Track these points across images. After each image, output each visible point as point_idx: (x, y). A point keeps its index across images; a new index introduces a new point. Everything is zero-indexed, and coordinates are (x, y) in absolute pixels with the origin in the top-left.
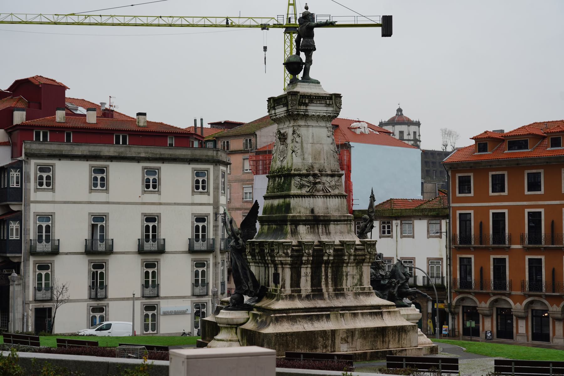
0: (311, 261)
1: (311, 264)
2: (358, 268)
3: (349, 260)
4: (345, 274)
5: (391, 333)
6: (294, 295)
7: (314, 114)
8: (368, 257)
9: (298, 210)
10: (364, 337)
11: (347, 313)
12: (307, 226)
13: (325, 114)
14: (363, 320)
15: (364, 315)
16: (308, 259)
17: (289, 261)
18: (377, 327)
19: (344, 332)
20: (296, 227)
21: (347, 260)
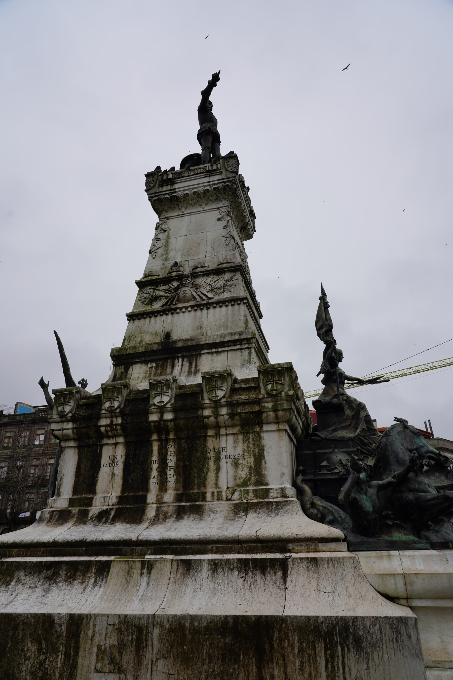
0: (119, 427)
1: (125, 437)
2: (248, 439)
3: (216, 418)
4: (212, 455)
5: (292, 646)
6: (70, 512)
8: (270, 405)
9: (139, 339)
11: (165, 560)
12: (147, 364)
14: (212, 585)
15: (220, 570)
16: (112, 422)
17: (70, 432)
18: (236, 618)
19: (110, 628)
20: (127, 370)
21: (212, 419)
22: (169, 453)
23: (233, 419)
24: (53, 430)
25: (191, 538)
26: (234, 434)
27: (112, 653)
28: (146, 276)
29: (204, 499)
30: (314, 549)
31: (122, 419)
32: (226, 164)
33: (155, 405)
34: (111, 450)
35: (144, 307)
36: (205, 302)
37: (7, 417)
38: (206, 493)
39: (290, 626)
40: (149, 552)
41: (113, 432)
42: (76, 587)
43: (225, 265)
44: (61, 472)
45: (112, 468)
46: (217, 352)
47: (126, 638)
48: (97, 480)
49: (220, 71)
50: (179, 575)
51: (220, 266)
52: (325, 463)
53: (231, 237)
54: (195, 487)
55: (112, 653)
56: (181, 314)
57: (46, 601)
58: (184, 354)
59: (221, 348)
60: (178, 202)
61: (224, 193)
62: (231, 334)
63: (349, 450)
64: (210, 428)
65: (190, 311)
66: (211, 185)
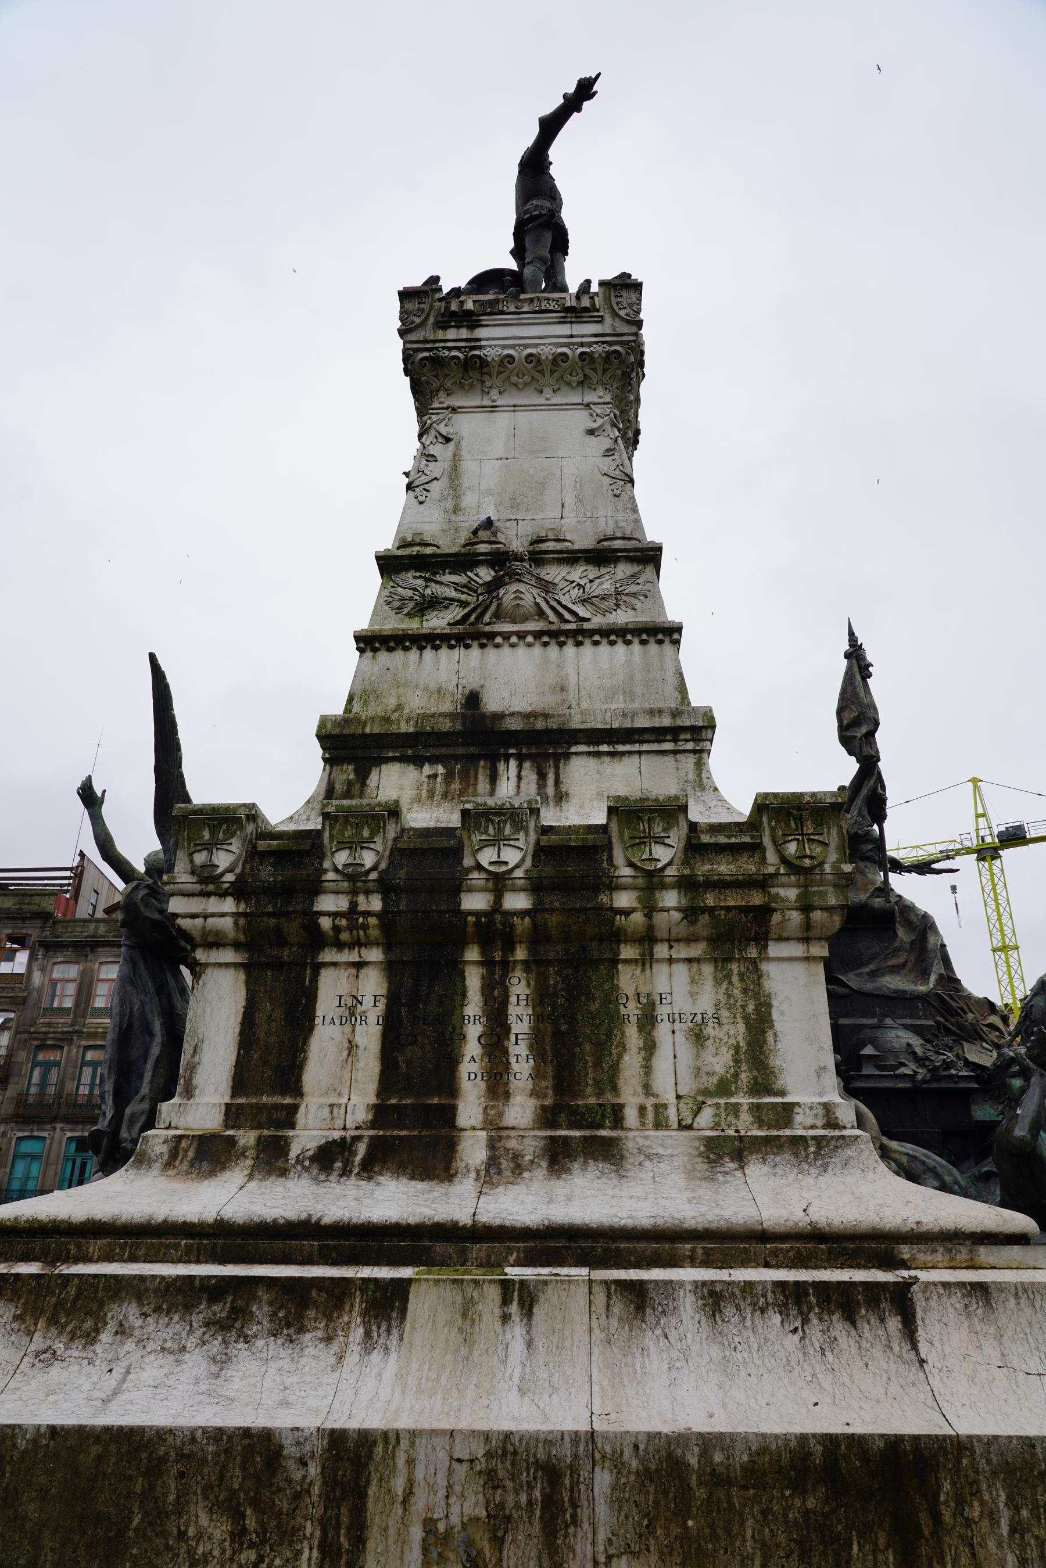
0: (373, 921)
1: (388, 947)
2: (728, 976)
3: (649, 916)
4: (632, 1010)
5: (992, 1517)
8: (791, 894)
9: (392, 702)
10: (686, 1537)
11: (569, 1281)
12: (422, 766)
14: (716, 1352)
15: (729, 1311)
16: (354, 905)
17: (227, 923)
18: (830, 1441)
19: (461, 1470)
20: (363, 776)
21: (638, 918)
22: (513, 999)
23: (693, 923)
24: (176, 916)
25: (629, 1223)
26: (689, 960)
27: (470, 1543)
28: (404, 544)
29: (618, 1122)
30: (966, 1261)
31: (384, 900)
32: (614, 301)
33: (479, 867)
34: (344, 980)
35: (402, 620)
36: (572, 626)
38: (621, 1107)
39: (983, 1464)
40: (512, 1258)
41: (355, 932)
42: (310, 1351)
43: (618, 544)
44: (196, 1033)
45: (348, 1028)
46: (612, 754)
47: (510, 1499)
48: (305, 1059)
49: (598, 75)
50: (614, 1322)
51: (605, 543)
52: (869, 1050)
53: (627, 479)
54: (589, 1091)
55: (470, 1543)
56: (506, 650)
57: (228, 1390)
58: (524, 751)
59: (624, 743)
60: (482, 374)
61: (605, 370)
62: (651, 712)
63: (918, 1022)
64: (626, 942)
65: (529, 645)
66: (573, 344)
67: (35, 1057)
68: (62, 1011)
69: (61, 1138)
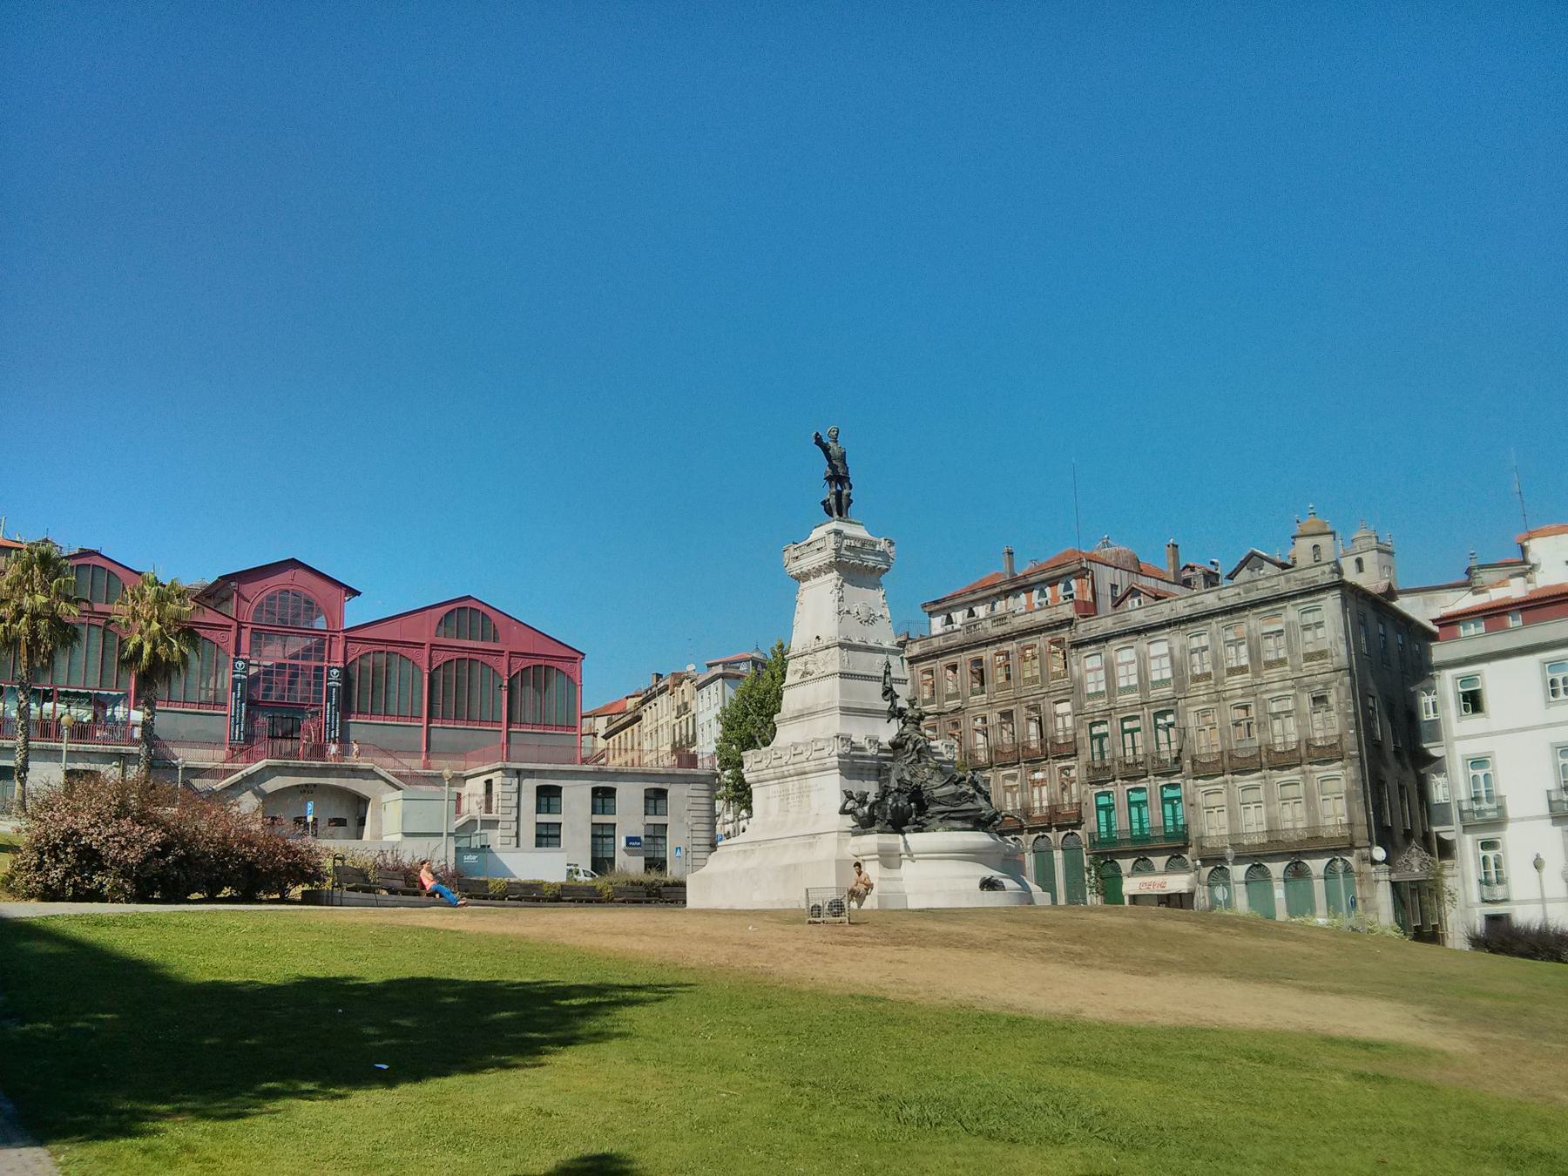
7: (809, 567)
13: (820, 564)
37: (918, 643)
67: (1091, 731)
68: (1098, 694)
69: (1156, 788)
